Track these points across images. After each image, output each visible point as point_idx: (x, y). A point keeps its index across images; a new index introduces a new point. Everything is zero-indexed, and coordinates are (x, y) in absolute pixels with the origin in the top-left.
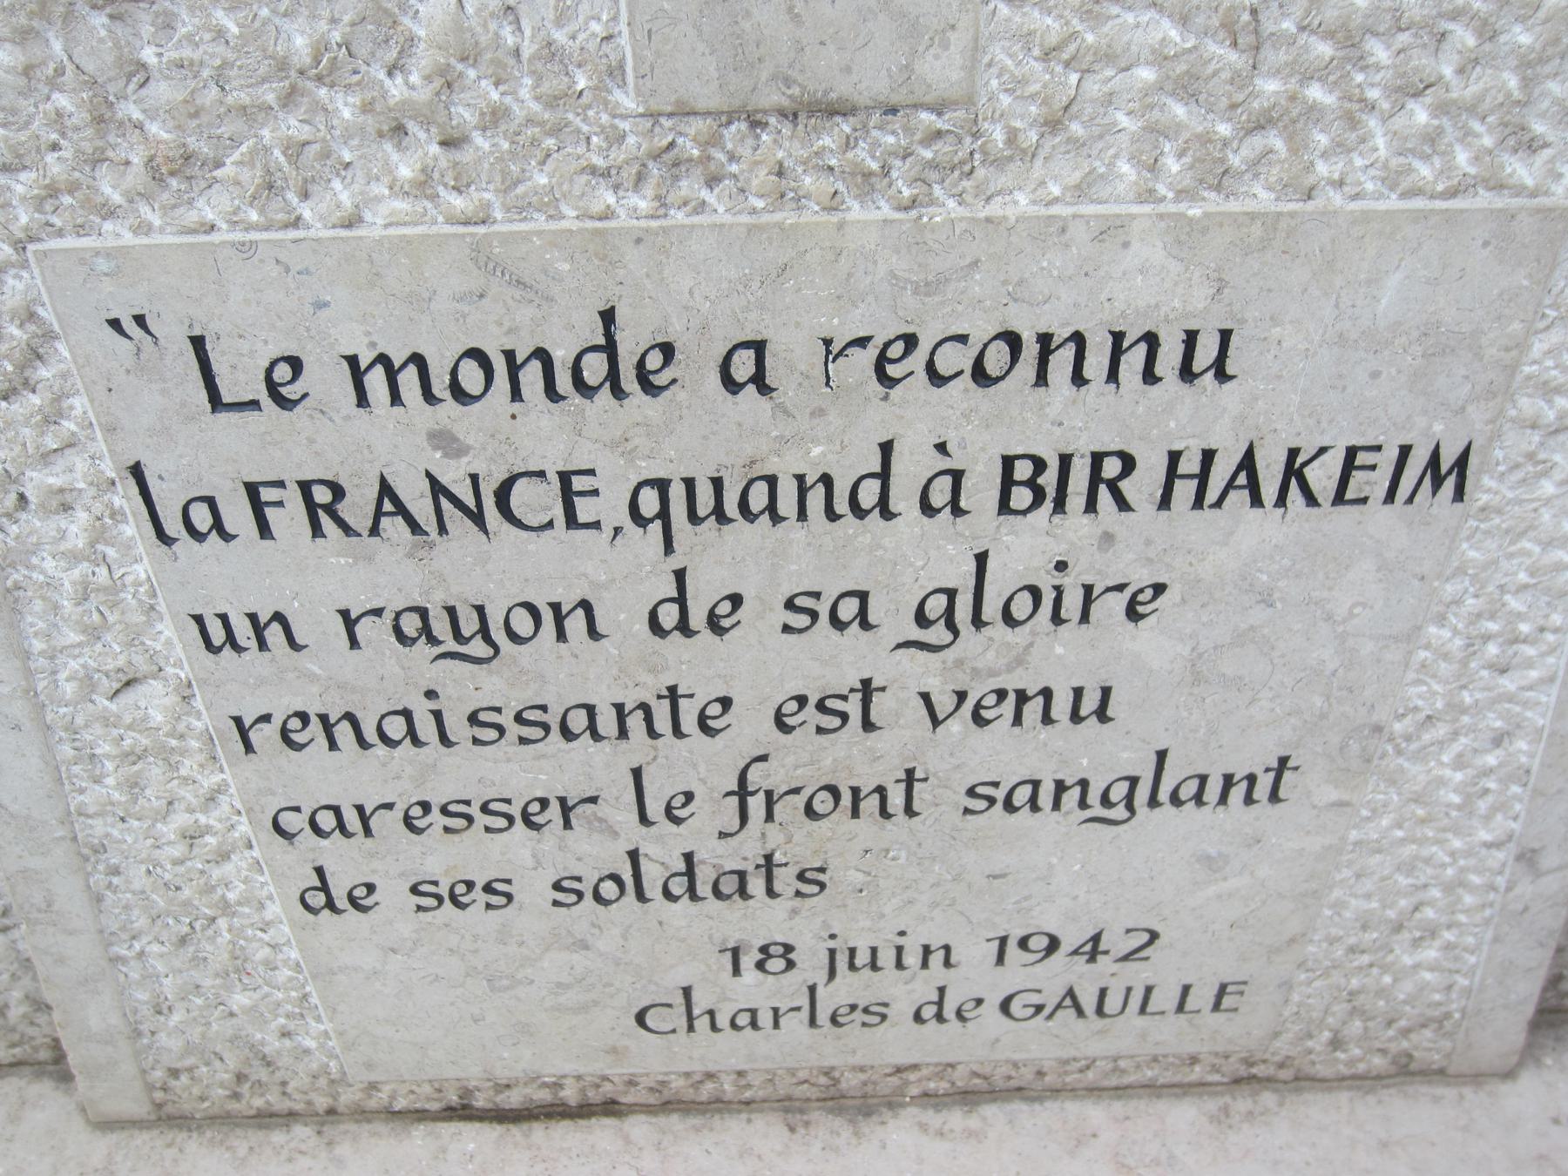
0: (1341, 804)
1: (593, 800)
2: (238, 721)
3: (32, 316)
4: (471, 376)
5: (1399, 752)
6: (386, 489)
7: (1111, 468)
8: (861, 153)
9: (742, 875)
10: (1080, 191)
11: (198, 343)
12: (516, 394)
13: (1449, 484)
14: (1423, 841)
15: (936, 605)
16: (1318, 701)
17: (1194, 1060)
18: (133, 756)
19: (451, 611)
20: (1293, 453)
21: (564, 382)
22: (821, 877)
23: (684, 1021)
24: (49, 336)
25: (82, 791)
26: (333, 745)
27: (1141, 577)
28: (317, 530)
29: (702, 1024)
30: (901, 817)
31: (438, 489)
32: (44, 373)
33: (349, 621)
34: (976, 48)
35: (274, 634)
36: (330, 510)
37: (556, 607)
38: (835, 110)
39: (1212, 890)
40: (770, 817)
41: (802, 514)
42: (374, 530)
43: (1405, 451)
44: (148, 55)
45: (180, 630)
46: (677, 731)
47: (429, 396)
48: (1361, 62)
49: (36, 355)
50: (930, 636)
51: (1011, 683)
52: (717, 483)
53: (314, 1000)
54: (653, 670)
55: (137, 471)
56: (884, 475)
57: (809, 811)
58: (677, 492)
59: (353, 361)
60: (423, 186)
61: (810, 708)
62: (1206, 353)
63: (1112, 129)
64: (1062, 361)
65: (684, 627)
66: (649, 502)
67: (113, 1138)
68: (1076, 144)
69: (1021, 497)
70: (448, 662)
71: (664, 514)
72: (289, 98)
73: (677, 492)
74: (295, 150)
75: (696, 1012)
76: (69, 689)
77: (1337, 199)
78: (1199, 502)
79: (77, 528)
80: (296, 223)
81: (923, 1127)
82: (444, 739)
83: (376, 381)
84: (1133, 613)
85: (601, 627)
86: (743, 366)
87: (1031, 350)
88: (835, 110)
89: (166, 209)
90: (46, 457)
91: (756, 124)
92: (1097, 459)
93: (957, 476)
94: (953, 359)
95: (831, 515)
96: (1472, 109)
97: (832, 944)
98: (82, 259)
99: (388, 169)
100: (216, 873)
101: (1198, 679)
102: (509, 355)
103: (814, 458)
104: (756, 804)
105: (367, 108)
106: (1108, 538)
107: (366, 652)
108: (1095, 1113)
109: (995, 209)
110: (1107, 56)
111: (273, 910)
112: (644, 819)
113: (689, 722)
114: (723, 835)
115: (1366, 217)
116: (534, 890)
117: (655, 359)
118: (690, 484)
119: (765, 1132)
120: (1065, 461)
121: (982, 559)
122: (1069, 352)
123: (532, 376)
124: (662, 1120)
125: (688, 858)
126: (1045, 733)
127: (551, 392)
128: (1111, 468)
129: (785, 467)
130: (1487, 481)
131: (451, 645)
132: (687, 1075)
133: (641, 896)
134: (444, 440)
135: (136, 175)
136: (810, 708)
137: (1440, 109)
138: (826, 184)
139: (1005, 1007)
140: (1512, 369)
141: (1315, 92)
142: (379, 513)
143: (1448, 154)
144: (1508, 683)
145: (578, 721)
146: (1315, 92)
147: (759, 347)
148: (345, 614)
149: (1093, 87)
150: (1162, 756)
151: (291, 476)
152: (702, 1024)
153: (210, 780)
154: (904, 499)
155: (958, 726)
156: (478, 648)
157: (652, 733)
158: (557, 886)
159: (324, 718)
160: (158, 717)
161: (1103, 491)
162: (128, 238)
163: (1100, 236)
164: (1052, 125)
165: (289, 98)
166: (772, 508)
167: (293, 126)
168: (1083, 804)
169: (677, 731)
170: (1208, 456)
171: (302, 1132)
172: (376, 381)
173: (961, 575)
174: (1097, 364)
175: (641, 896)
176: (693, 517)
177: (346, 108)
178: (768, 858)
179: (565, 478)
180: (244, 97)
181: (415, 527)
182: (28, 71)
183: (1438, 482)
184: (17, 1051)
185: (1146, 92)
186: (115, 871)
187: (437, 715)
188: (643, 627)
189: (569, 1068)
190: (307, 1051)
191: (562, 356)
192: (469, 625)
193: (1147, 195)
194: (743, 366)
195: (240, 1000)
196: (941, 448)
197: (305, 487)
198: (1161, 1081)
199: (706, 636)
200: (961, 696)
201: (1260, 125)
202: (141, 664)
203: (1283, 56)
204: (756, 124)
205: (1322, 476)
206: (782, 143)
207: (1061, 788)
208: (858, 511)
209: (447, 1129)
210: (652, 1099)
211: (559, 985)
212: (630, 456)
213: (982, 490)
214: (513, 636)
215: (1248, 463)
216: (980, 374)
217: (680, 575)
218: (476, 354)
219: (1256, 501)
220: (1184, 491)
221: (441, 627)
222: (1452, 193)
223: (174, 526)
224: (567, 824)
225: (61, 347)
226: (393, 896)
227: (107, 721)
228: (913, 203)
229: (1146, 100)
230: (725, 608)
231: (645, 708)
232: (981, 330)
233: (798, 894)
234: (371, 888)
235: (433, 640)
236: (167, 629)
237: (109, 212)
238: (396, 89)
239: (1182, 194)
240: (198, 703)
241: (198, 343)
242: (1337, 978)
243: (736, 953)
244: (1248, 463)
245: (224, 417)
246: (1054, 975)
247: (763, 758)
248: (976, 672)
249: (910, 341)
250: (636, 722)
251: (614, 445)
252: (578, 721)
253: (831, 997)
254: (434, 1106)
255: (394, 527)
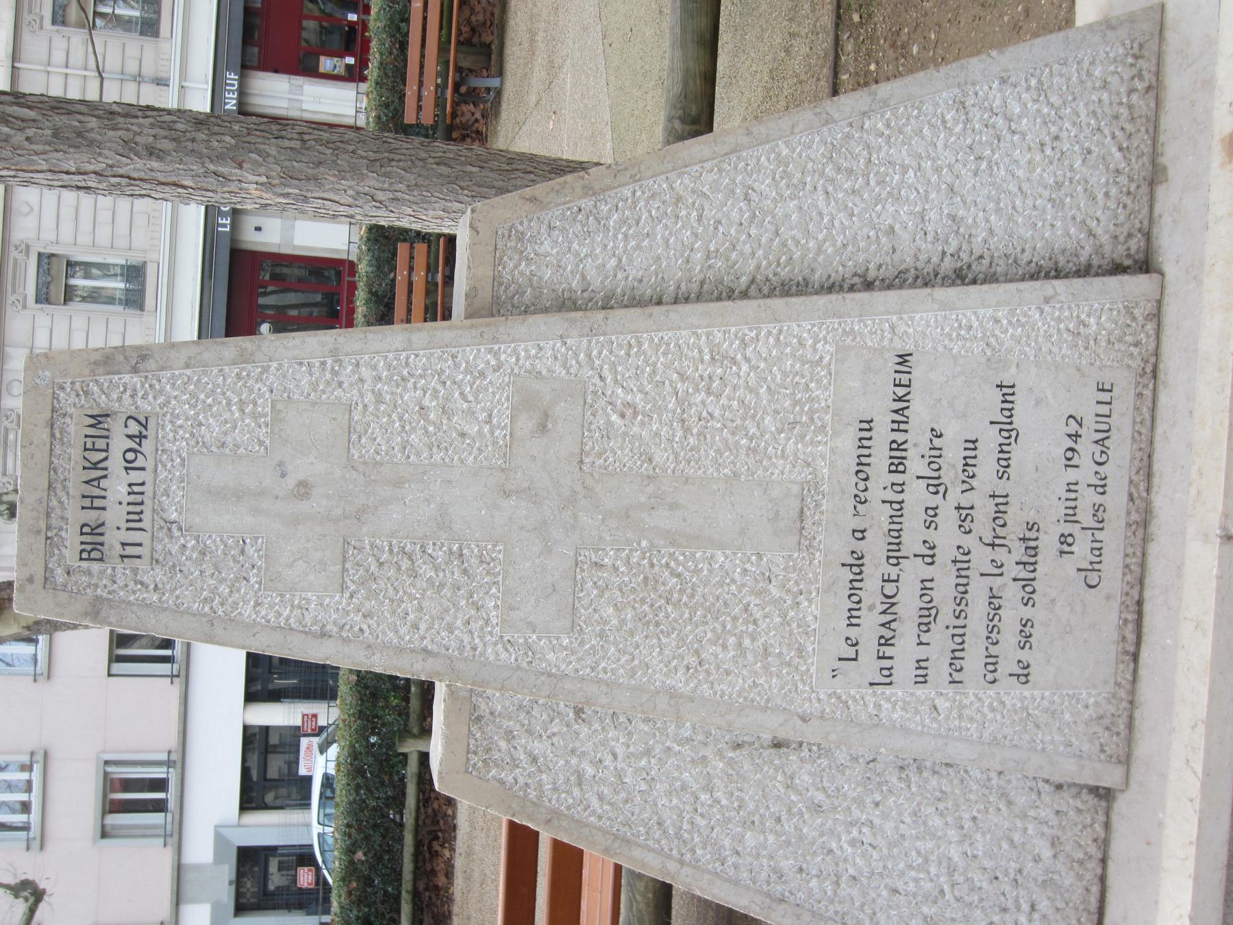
0: (1018, 365)
1: (991, 589)
2: (950, 682)
3: (830, 695)
4: (855, 599)
5: (999, 351)
6: (883, 625)
7: (895, 446)
8: (811, 506)
9: (1027, 548)
10: (823, 458)
11: (840, 659)
12: (861, 589)
13: (906, 358)
14: (1037, 336)
15: (932, 489)
16: (976, 380)
17: (1140, 395)
18: (961, 717)
19: (920, 616)
20: (894, 400)
21: (859, 577)
22: (1031, 524)
23: (1095, 573)
24: (835, 692)
25: (972, 736)
26: (963, 658)
27: (929, 435)
28: (892, 645)
29: (1096, 566)
30: (1008, 499)
31: (884, 612)
32: (844, 698)
33: (920, 644)
34: (791, 482)
35: (923, 664)
36: (887, 640)
37: (922, 589)
38: (802, 511)
39: (1051, 400)
40: (1004, 538)
41: (901, 523)
42: (894, 631)
43: (896, 372)
44: (777, 651)
45: (919, 688)
46: (968, 561)
47: (859, 609)
48: (800, 400)
49: (839, 698)
50: (942, 489)
51: (961, 468)
52: (889, 544)
53: (1071, 692)
54: (946, 566)
55: (871, 684)
56: (891, 503)
57: (1003, 526)
58: (891, 554)
59: (848, 625)
60: (810, 601)
61: (964, 524)
62: (866, 426)
63: (811, 452)
64: (864, 460)
65: (932, 556)
66: (893, 561)
67: (1132, 781)
68: (814, 459)
69: (901, 468)
70: (937, 619)
71: (897, 558)
72: (789, 625)
73: (891, 554)
74: (799, 626)
75: (1090, 568)
76: (935, 725)
77: (830, 400)
78: (907, 422)
79: (886, 706)
80: (815, 630)
81: (1157, 493)
82: (964, 627)
83: (854, 621)
84: (940, 436)
85: (930, 578)
86: (859, 535)
87: (861, 468)
88: (802, 511)
89: (809, 657)
90: (865, 705)
91: (803, 528)
92: (891, 449)
93: (893, 484)
94: (862, 486)
95: (901, 516)
96: (811, 374)
97: (1062, 521)
98: (817, 679)
99: (805, 607)
100: (1009, 707)
101: (965, 416)
102: (850, 589)
103: (885, 520)
104: (997, 541)
105: (792, 609)
106: (915, 445)
107: (931, 642)
108: (1159, 430)
109: (826, 477)
110: (795, 454)
111: (1026, 693)
112: (1001, 575)
113: (966, 558)
114: (1010, 552)
115: (835, 394)
116: (1027, 612)
117: (855, 556)
118: (889, 551)
119: (1153, 549)
120: (891, 457)
121: (918, 477)
122: (862, 459)
123: (856, 584)
124: (1146, 585)
125: (1017, 563)
126: (980, 458)
127: (861, 581)
128: (895, 446)
129: (886, 527)
130: (907, 348)
131: (932, 619)
132: (1124, 574)
133: (1034, 579)
134: (872, 608)
135: (801, 661)
136: (964, 524)
137: (811, 381)
138: (817, 514)
139: (1100, 464)
140: (875, 350)
141: (806, 409)
142: (889, 628)
143: (821, 377)
144: (976, 324)
145: (961, 589)
146: (806, 409)
147: (854, 531)
148: (918, 644)
149: (802, 457)
150: (992, 423)
151: (877, 647)
152: (1096, 566)
153: (972, 698)
154: (899, 497)
155: (974, 483)
156: (933, 612)
157: (968, 569)
158: (1026, 604)
159: (952, 659)
160: (947, 704)
161: (901, 447)
162: (814, 667)
163: (834, 453)
164: (809, 465)
165: (789, 625)
166: (898, 531)
167: (794, 625)
168: (1009, 444)
169: (968, 561)
170: (893, 422)
171: (1137, 714)
172: (854, 621)
173: (923, 483)
174: (866, 452)
175: (1034, 579)
176: (899, 550)
177: (792, 614)
178: (1020, 539)
179: (884, 581)
180: (787, 635)
181: (894, 620)
182: (778, 676)
183: (906, 361)
184: (1100, 812)
185: (803, 445)
186: (1005, 738)
187: (954, 627)
188: (931, 567)
189: (1115, 614)
190: (1096, 702)
191: (852, 577)
192: (926, 613)
193: (826, 443)
194: (859, 535)
195: (1067, 716)
196: (885, 488)
197: (880, 645)
198: (1150, 405)
199: (935, 551)
200: (963, 482)
201: (812, 420)
202: (929, 703)
203: (798, 417)
204: (803, 528)
205: (901, 391)
206: (808, 523)
207: (1002, 451)
208: (901, 509)
209: (1141, 662)
210: (1138, 588)
211: (1071, 611)
212: (880, 564)
213: (898, 478)
214: (931, 601)
215: (896, 412)
216: (866, 479)
217: (915, 556)
218: (850, 596)
219: (908, 407)
220: (902, 426)
221: (926, 620)
222: (831, 374)
223: (888, 680)
224: (1000, 598)
225: (839, 691)
226: (1025, 655)
227: (947, 718)
228: (823, 495)
229: (805, 445)
230: (927, 545)
231: (958, 570)
232: (855, 479)
233: (1038, 531)
234: (1019, 661)
235: (929, 623)
236: (919, 693)
237: (808, 670)
238: (789, 602)
239: (826, 436)
240: (944, 692)
241: (840, 659)
242: (1100, 351)
243: (1062, 552)
244: (896, 412)
245: (859, 658)
246: (1086, 448)
247: (981, 539)
248: (955, 478)
249: (856, 496)
250: (963, 573)
251: (876, 568)
252: (961, 589)
253: (1088, 521)
254: (1132, 665)
255: (893, 625)
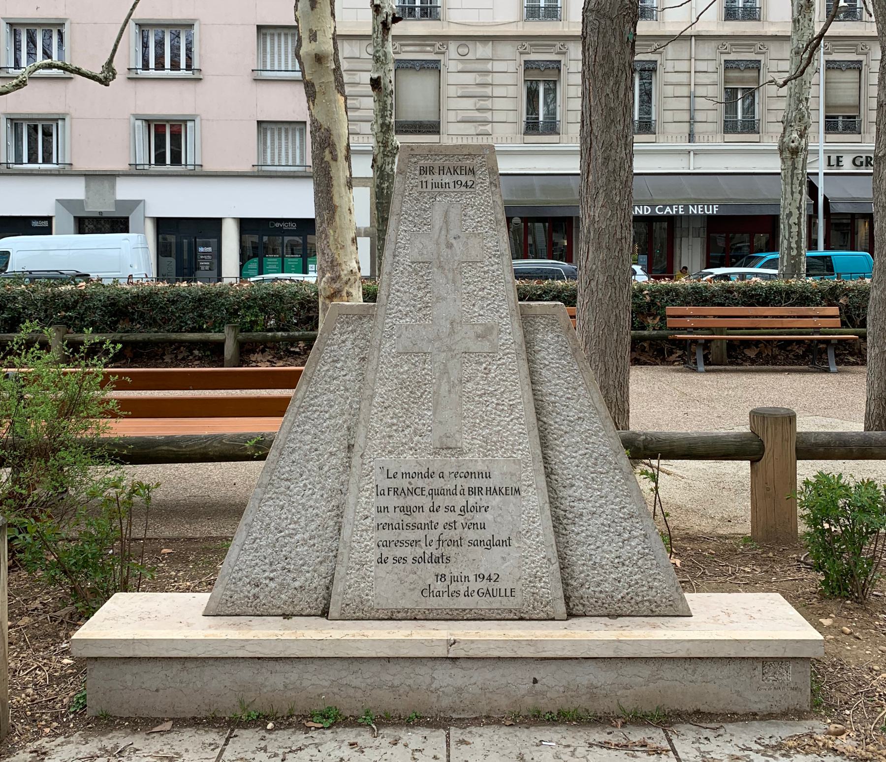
10: (473, 457)
15: (462, 508)
18: (363, 530)
27: (486, 505)
29: (431, 594)
31: (408, 489)
38: (451, 448)
39: (505, 565)
60: (412, 455)
62: (488, 475)
64: (473, 475)
65: (433, 511)
66: (431, 493)
69: (471, 493)
86: (441, 476)
88: (451, 448)
90: (368, 484)
94: (462, 475)
104: (441, 542)
116: (410, 560)
123: (420, 475)
126: (477, 531)
132: (428, 610)
144: (535, 525)
154: (458, 493)
156: (409, 513)
164: (469, 450)
167: (402, 448)
174: (477, 476)
189: (410, 606)
194: (441, 476)
205: (503, 491)
206: (445, 451)
213: (466, 492)
220: (489, 492)
223: (379, 494)
226: (390, 560)
227: (362, 524)
232: (465, 471)
236: (373, 509)
246: (484, 585)
252: (419, 527)
